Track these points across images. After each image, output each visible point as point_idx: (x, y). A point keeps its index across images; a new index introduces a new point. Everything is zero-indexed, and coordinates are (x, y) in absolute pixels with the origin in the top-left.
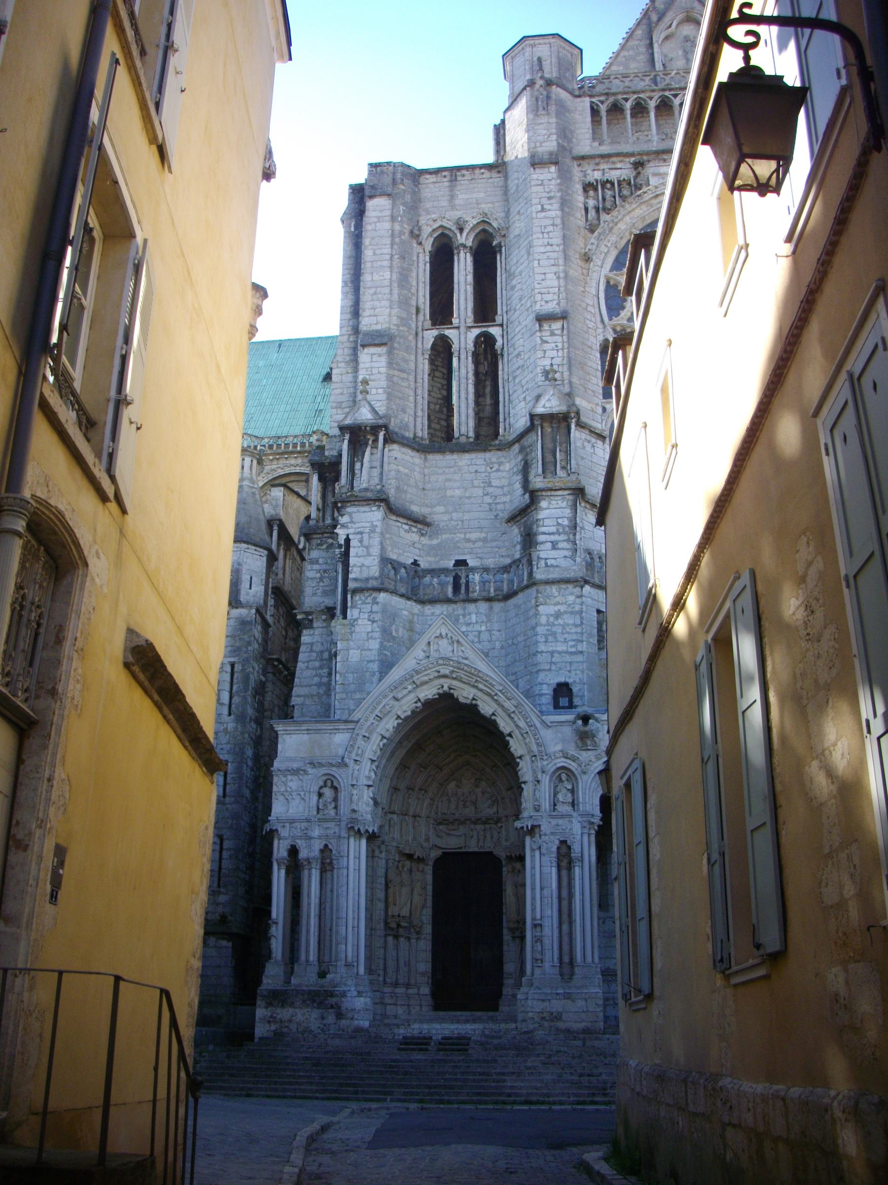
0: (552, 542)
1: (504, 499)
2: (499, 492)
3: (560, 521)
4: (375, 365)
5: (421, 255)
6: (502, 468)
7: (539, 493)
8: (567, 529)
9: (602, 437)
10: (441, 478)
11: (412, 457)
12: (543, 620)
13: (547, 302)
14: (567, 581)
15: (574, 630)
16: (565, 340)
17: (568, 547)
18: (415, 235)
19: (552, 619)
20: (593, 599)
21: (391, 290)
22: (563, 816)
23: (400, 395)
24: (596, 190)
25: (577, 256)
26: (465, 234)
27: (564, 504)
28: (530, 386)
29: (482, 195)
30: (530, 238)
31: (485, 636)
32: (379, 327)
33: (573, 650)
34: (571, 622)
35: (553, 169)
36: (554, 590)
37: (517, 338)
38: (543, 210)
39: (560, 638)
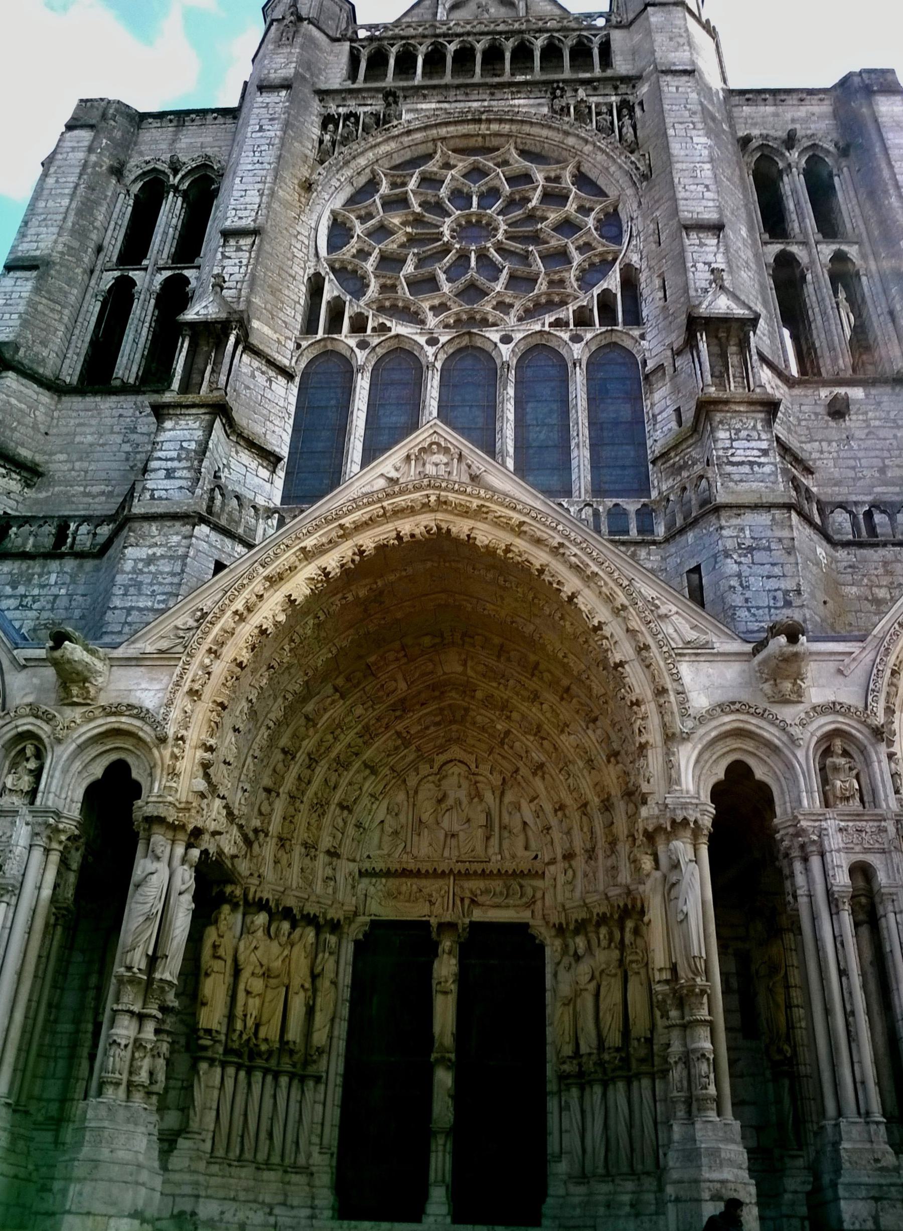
0: (167, 470)
3: (185, 444)
4: (18, 289)
5: (122, 196)
7: (166, 411)
9: (289, 376)
10: (72, 422)
11: (38, 394)
12: (128, 565)
13: (240, 218)
14: (174, 517)
15: (169, 580)
16: (253, 255)
17: (188, 475)
18: (118, 171)
19: (140, 565)
20: (211, 545)
21: (65, 218)
23: (43, 326)
25: (296, 182)
26: (179, 176)
29: (210, 139)
31: (62, 603)
32: (38, 253)
34: (167, 569)
35: (283, 93)
36: (154, 528)
38: (261, 129)
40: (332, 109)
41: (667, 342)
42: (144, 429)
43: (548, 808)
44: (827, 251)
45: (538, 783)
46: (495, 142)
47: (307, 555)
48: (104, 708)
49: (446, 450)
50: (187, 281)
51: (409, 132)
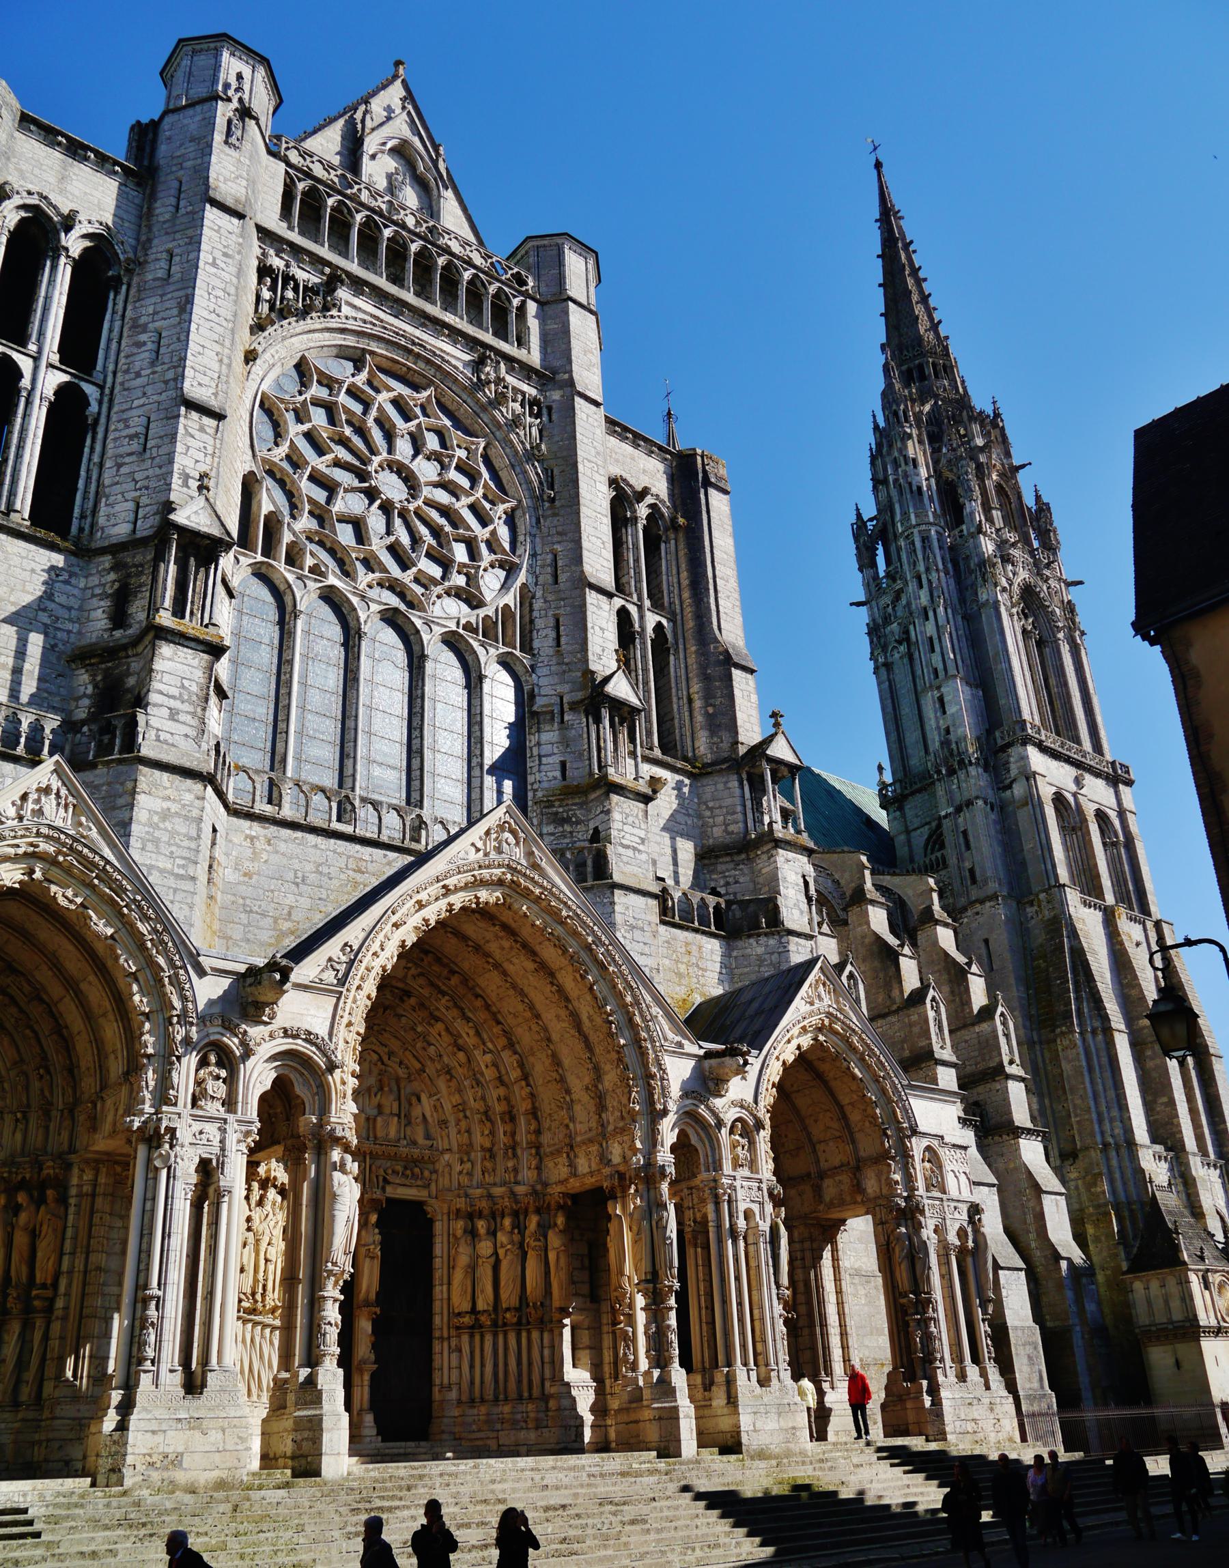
1: (69, 626)
2: (62, 613)
3: (186, 683)
6: (73, 581)
8: (194, 698)
19: (156, 819)
22: (211, 1119)
24: (274, 281)
27: (196, 662)
28: (152, 484)
30: (189, 291)
33: (182, 872)
34: (184, 830)
35: (235, 221)
37: (135, 412)
39: (165, 850)
40: (277, 262)
41: (559, 689)
42: (61, 599)
43: (448, 1107)
44: (652, 619)
45: (441, 1084)
46: (417, 379)
47: (421, 905)
48: (285, 1031)
49: (512, 832)
50: (84, 400)
51: (343, 331)
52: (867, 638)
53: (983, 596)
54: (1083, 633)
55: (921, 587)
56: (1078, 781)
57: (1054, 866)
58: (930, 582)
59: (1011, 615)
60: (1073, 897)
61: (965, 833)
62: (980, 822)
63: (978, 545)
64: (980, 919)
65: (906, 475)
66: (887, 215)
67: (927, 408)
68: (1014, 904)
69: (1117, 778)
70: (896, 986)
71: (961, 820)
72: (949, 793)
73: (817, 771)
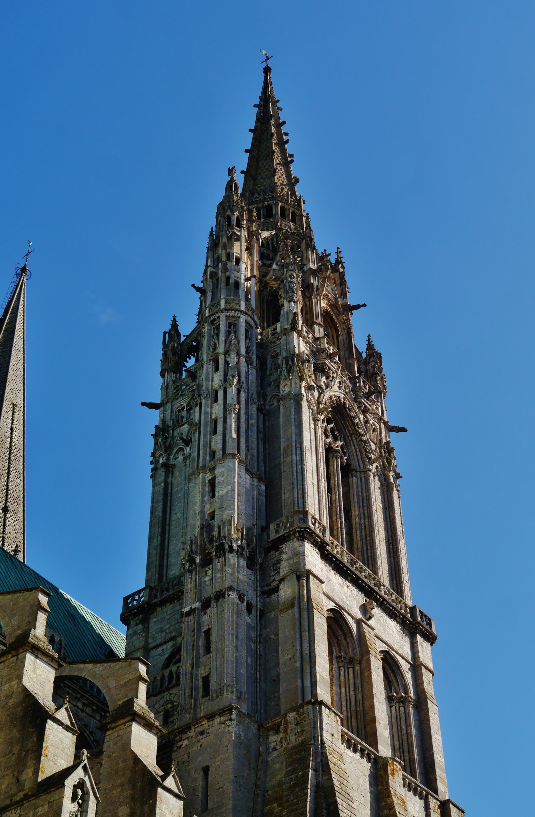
52: (152, 440)
53: (285, 388)
54: (398, 476)
55: (217, 369)
56: (364, 609)
57: (314, 684)
58: (227, 363)
59: (316, 420)
60: (331, 728)
61: (208, 633)
62: (229, 622)
63: (289, 342)
64: (204, 740)
65: (225, 269)
66: (266, 98)
67: (265, 234)
68: (254, 728)
69: (415, 626)
70: (31, 763)
71: (206, 618)
72: (200, 585)
73: (67, 596)
